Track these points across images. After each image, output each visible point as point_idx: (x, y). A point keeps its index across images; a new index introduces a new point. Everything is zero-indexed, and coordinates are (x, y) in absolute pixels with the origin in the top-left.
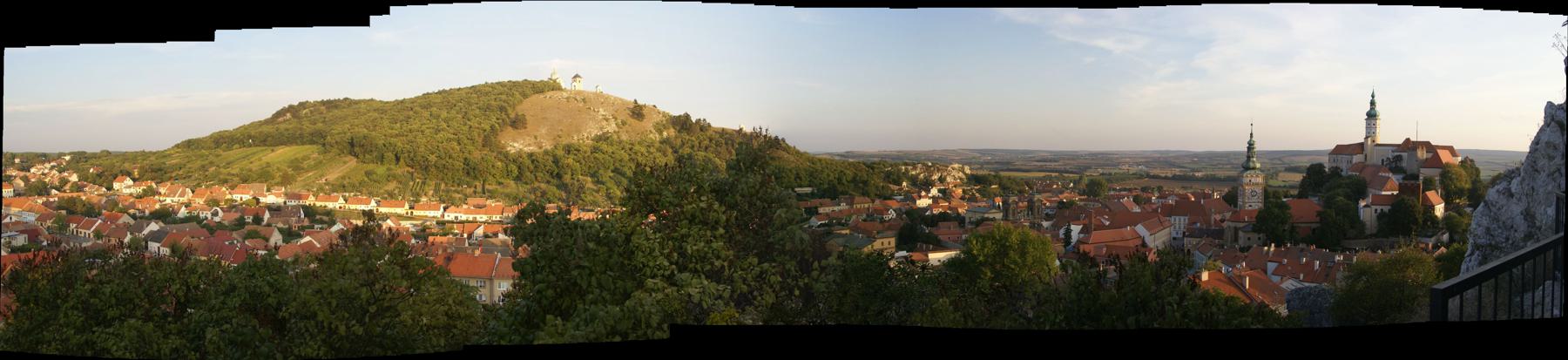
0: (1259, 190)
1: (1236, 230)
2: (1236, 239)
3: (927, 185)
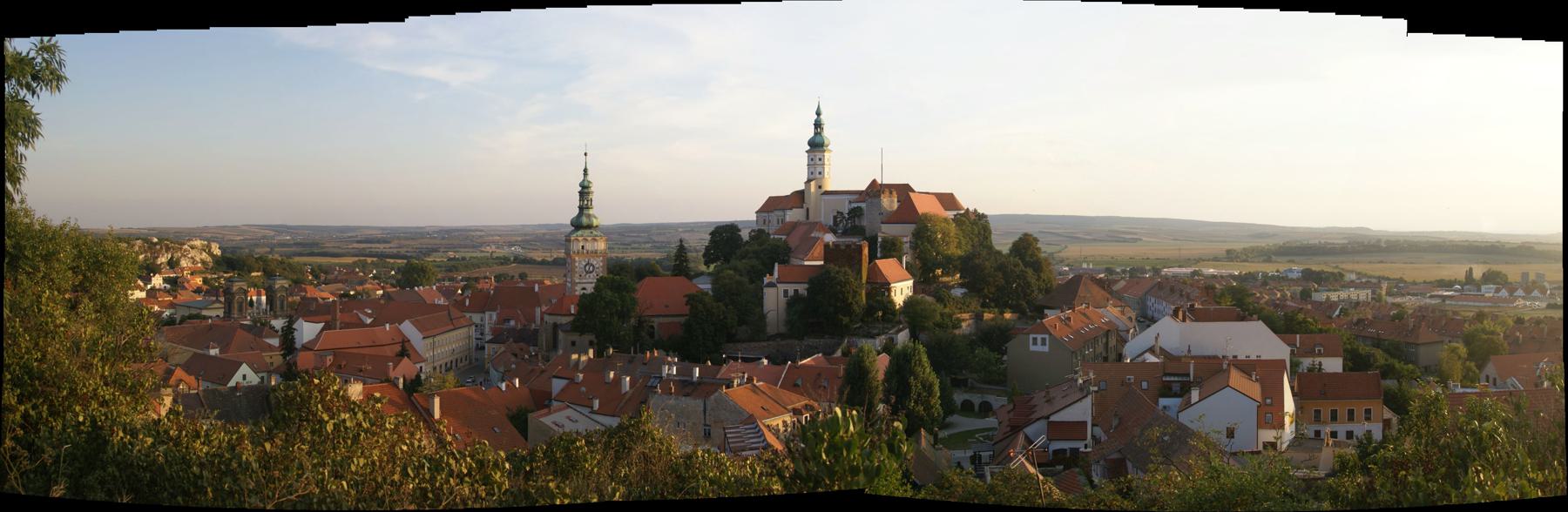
1: (555, 326)
3: (150, 269)
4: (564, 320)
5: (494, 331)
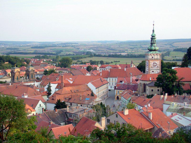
0: (158, 63)
1: (145, 85)
2: (145, 90)
4: (148, 83)
5: (117, 85)
